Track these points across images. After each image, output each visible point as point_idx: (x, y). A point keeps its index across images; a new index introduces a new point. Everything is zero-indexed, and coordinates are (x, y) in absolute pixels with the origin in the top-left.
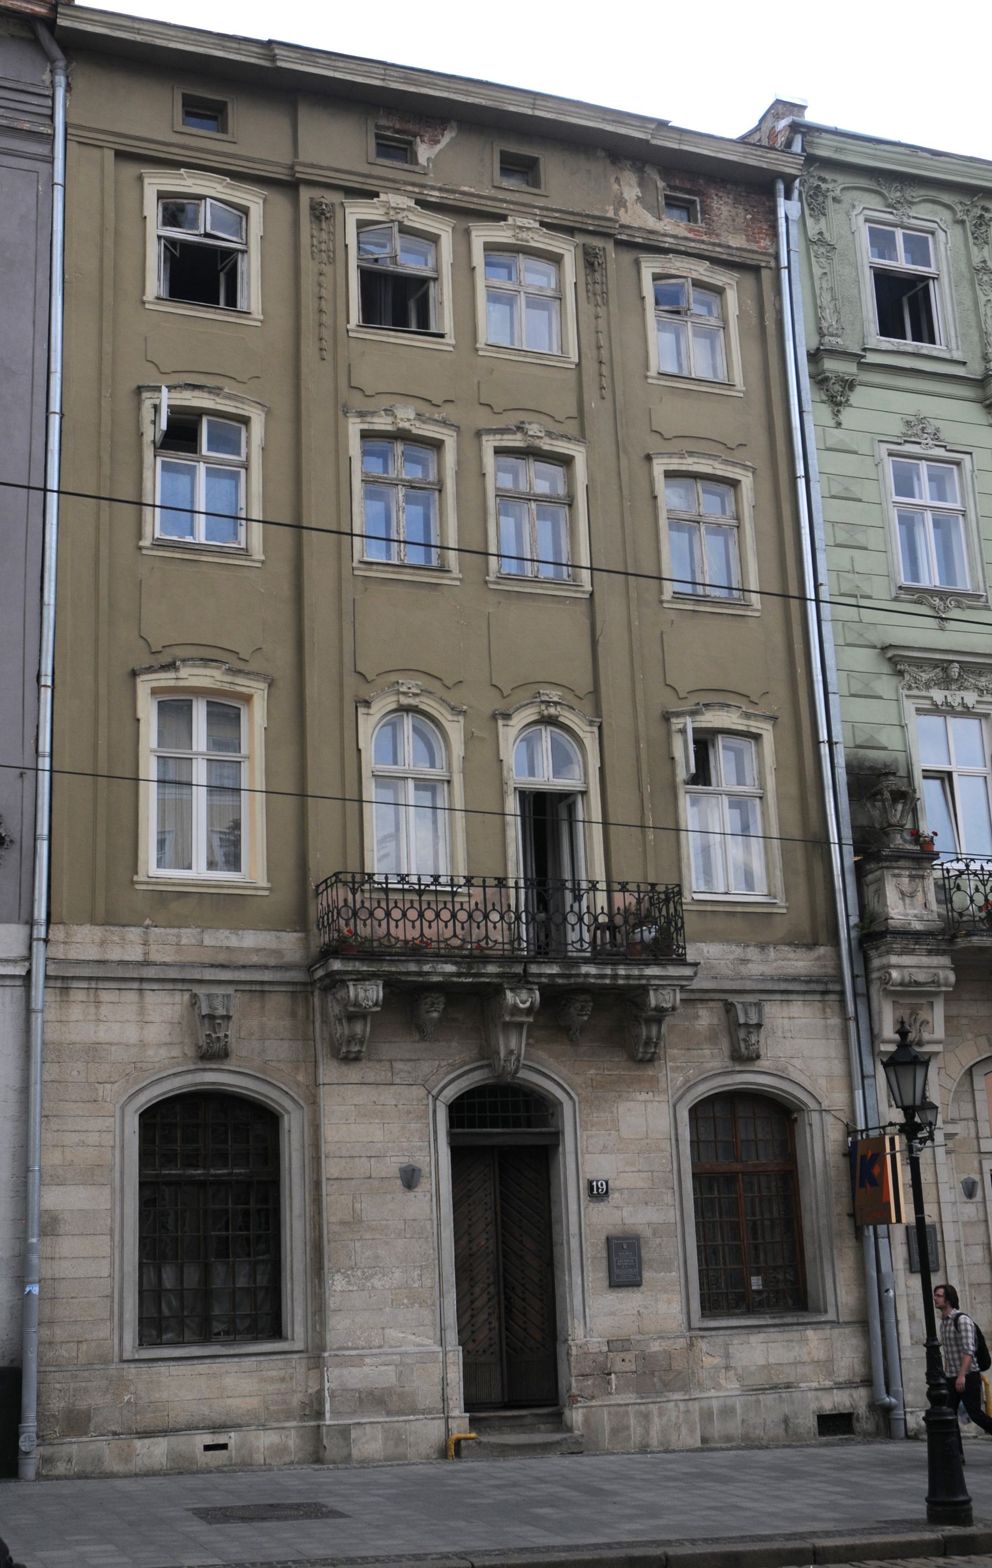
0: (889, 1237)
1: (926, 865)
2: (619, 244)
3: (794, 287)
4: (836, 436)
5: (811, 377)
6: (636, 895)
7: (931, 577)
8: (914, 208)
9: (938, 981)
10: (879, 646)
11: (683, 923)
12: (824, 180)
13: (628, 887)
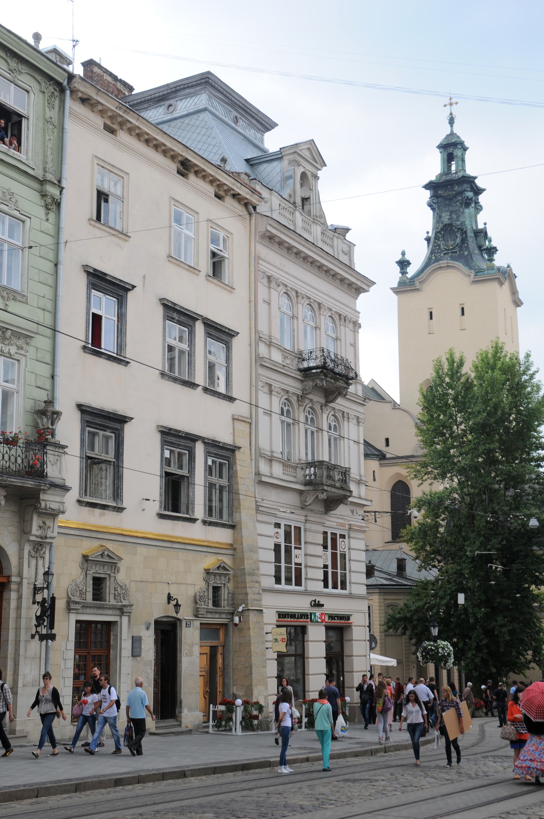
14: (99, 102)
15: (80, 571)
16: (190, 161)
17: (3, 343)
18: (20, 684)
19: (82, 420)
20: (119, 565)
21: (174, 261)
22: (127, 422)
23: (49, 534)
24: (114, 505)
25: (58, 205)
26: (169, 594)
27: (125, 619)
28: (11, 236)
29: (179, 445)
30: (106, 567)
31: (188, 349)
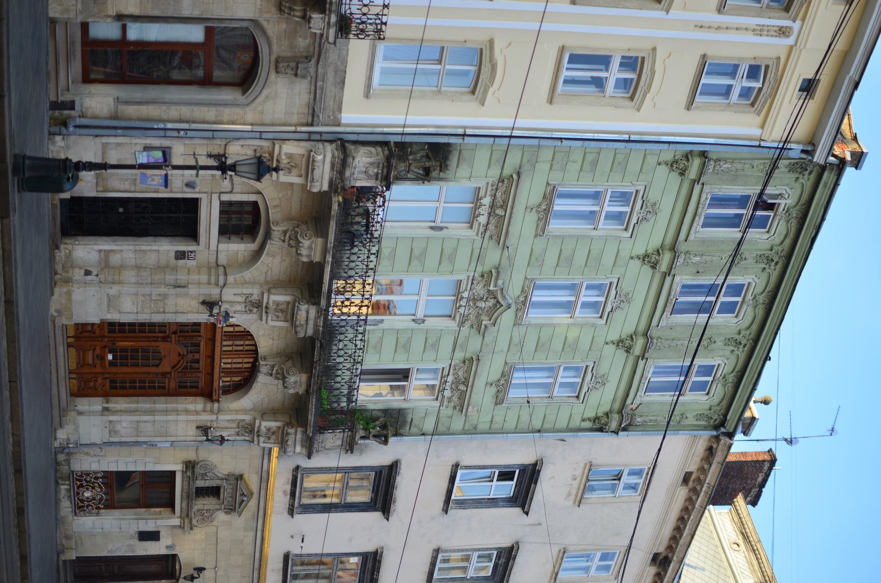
0: (165, 137)
1: (384, 183)
2: (791, 48)
3: (747, 148)
4: (652, 160)
5: (691, 151)
6: (381, 13)
7: (560, 205)
8: (785, 223)
9: (313, 182)
10: (520, 171)
11: (361, 39)
12: (810, 173)
13: (386, 9)
14: (711, 465)
15: (226, 473)
16: (669, 566)
17: (452, 383)
18: (112, 418)
19: (382, 467)
20: (233, 514)
21: (561, 555)
22: (384, 515)
23: (262, 439)
24: (296, 505)
25: (601, 430)
26: (204, 569)
27: (176, 522)
28: (562, 385)
29: (364, 572)
30: (230, 499)
31: (468, 577)
